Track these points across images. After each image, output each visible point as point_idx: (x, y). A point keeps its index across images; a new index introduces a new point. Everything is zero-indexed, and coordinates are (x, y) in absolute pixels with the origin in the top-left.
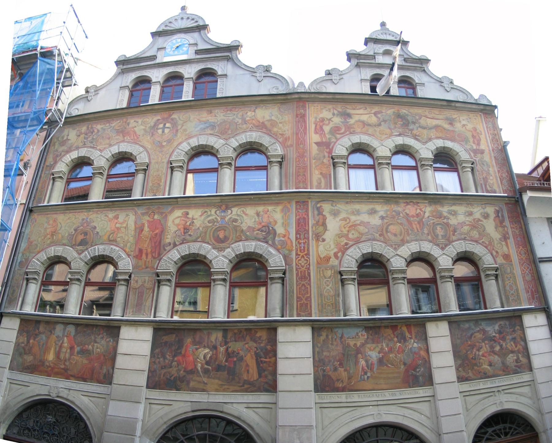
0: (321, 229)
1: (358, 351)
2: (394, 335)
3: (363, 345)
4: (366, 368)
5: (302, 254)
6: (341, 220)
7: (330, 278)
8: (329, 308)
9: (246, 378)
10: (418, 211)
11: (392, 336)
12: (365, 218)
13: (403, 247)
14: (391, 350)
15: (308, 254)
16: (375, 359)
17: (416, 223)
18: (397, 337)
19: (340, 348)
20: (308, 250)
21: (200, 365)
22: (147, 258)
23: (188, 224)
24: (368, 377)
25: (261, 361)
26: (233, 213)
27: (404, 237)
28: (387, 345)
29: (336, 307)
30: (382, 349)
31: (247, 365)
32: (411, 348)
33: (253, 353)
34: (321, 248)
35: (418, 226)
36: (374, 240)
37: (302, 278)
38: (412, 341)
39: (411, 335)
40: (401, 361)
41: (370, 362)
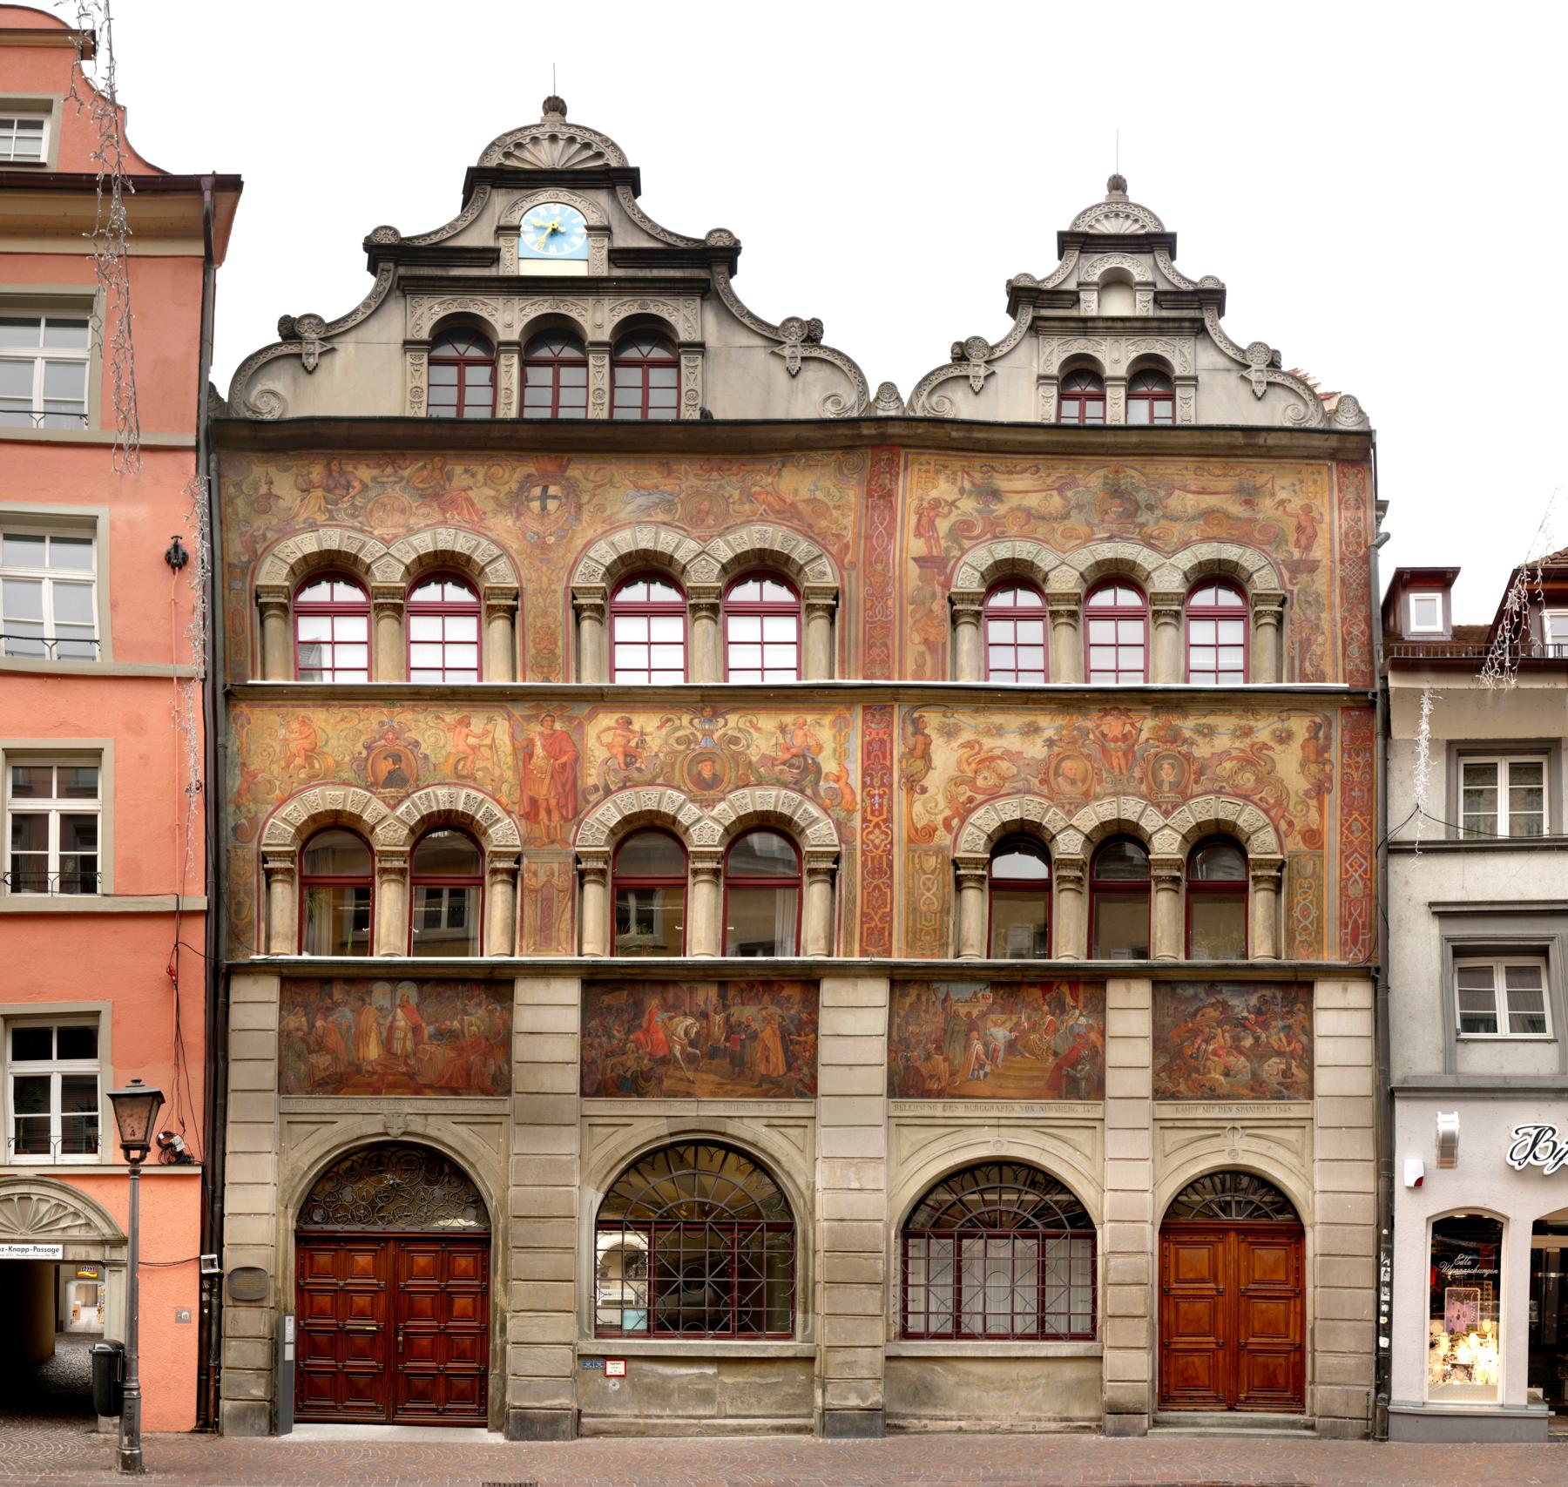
3: (983, 1015)
5: (875, 820)
7: (933, 872)
10: (1128, 727)
12: (1012, 742)
15: (889, 820)
20: (890, 810)
28: (1029, 1018)
30: (1018, 1024)
35: (1123, 762)
36: (1029, 792)
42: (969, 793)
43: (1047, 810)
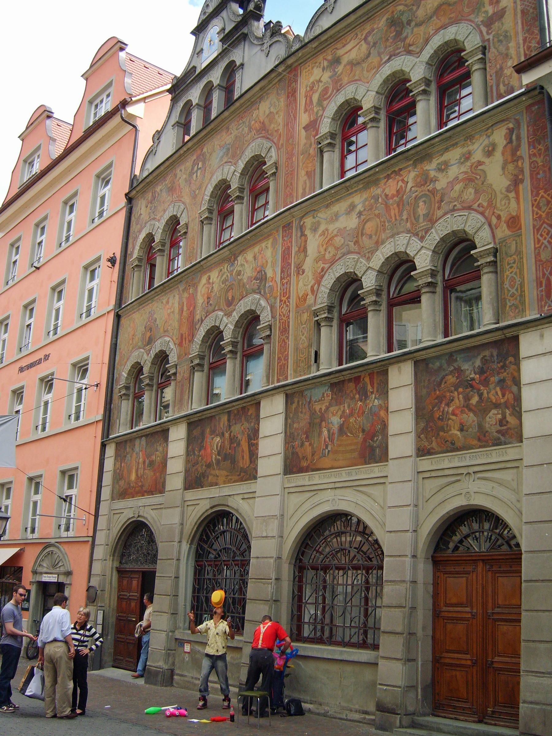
1: (323, 418)
3: (327, 408)
6: (320, 235)
11: (354, 392)
19: (307, 416)
28: (349, 406)
30: (344, 412)
34: (301, 284)
38: (374, 396)
42: (322, 265)
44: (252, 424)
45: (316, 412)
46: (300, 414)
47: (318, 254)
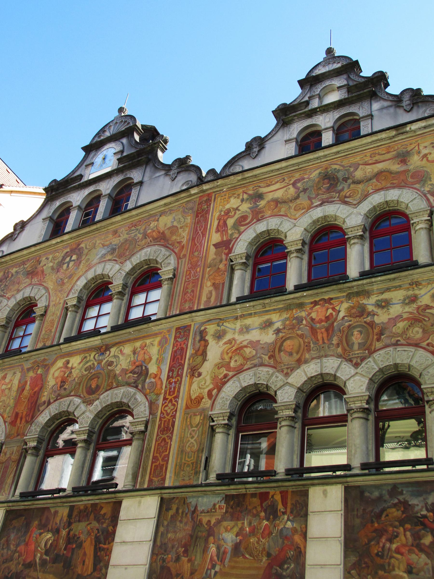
0: (200, 359)
1: (211, 532)
2: (262, 507)
3: (219, 522)
4: (215, 558)
5: (170, 397)
6: (226, 343)
7: (197, 426)
8: (188, 469)
9: (80, 572)
10: (330, 311)
11: (259, 509)
12: (255, 335)
13: (298, 371)
14: (253, 532)
15: (177, 397)
16: (230, 544)
17: (323, 330)
18: (265, 511)
19: (189, 527)
20: (179, 392)
21: (39, 555)
22: (20, 423)
23: (66, 375)
24: (216, 573)
25: (100, 548)
26: (111, 354)
27: (302, 355)
28: (250, 523)
29: (196, 467)
30: (242, 529)
31: (85, 554)
32: (282, 529)
33: (93, 537)
34: (195, 386)
35: (325, 335)
36: (262, 365)
37: (164, 430)
38: (286, 517)
39: (286, 508)
40: (264, 549)
41: (222, 549)
42: (225, 372)
43: (272, 375)
44: (105, 525)
45: (202, 524)
46: (178, 523)
47: (221, 361)
